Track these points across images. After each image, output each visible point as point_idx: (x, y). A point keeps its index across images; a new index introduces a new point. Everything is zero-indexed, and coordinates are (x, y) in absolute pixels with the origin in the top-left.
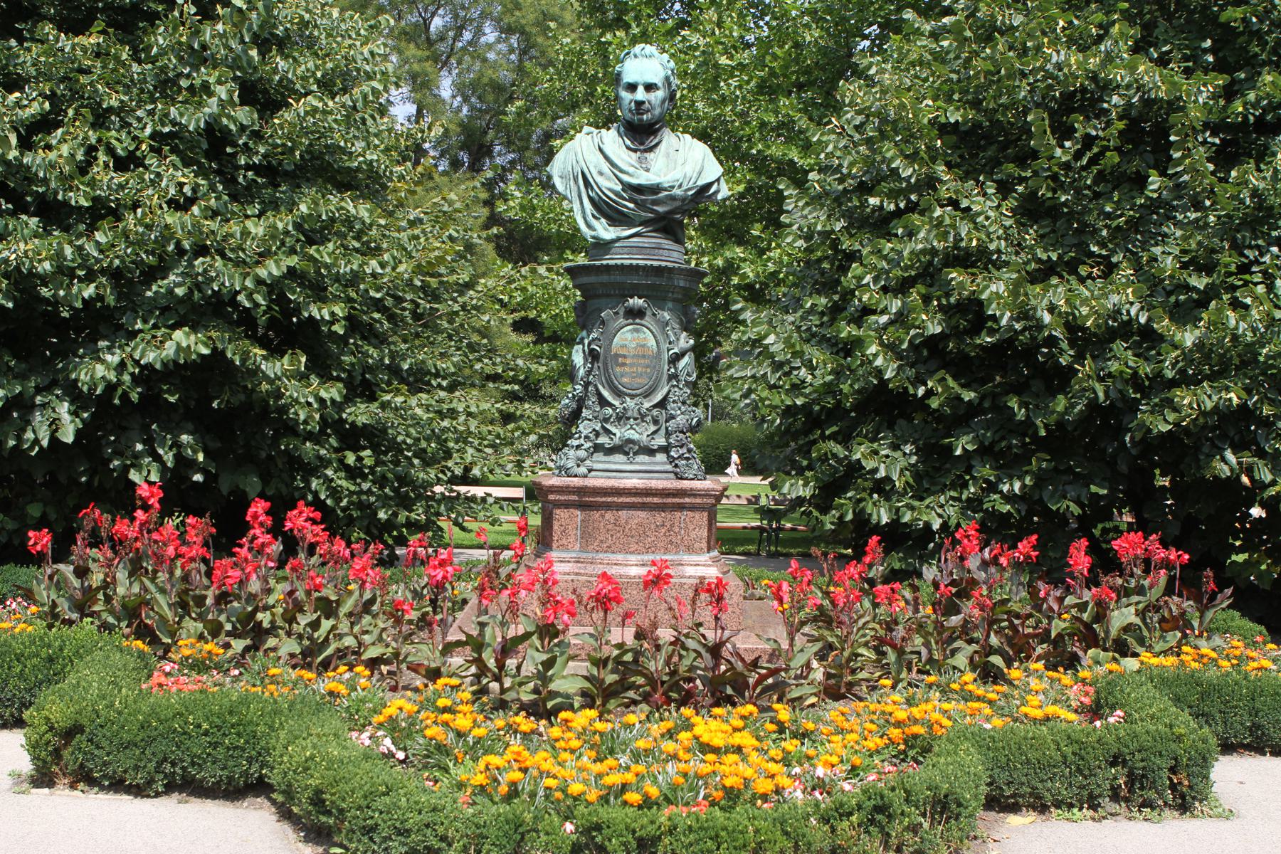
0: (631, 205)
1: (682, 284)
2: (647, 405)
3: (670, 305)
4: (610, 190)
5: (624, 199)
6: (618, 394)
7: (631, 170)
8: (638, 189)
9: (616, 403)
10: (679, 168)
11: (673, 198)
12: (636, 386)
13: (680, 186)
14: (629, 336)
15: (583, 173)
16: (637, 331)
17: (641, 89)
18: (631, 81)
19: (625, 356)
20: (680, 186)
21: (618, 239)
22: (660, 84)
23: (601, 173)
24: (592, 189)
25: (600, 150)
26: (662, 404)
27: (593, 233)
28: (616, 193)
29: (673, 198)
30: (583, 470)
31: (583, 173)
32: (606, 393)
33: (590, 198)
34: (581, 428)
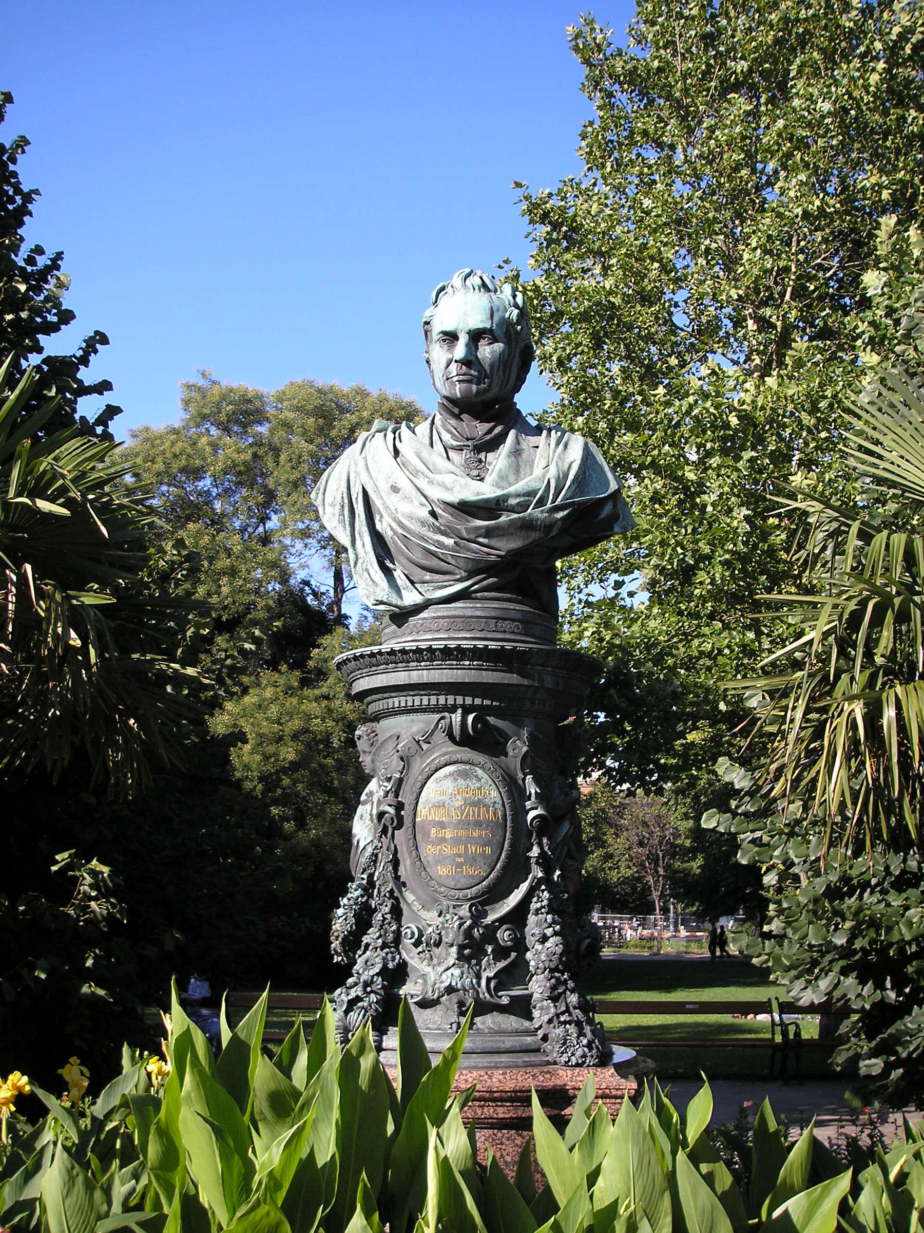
0: (450, 542)
2: (489, 920)
4: (411, 517)
10: (538, 471)
11: (527, 525)
12: (464, 882)
13: (541, 502)
14: (449, 786)
15: (365, 492)
16: (465, 775)
17: (463, 339)
18: (449, 328)
19: (442, 825)
20: (541, 502)
23: (395, 489)
24: (382, 517)
25: (397, 453)
26: (518, 917)
28: (423, 523)
31: (365, 492)
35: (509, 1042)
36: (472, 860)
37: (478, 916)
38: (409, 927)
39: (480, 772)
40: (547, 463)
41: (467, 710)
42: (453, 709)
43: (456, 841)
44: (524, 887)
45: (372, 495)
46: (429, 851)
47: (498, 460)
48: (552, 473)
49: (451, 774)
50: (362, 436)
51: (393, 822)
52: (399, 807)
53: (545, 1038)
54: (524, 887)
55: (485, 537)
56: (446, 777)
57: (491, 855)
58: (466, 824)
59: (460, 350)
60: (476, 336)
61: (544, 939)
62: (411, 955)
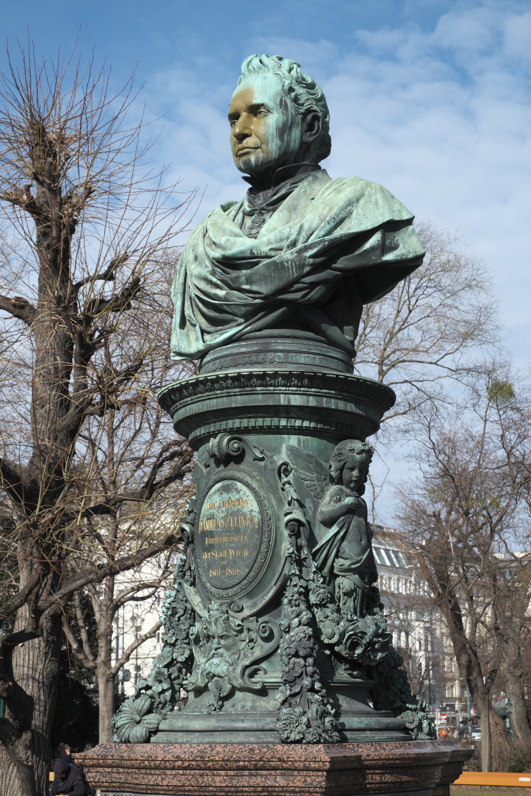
13: (294, 244)
16: (226, 489)
22: (270, 104)
29: (279, 267)
39: (239, 485)
49: (219, 490)
55: (247, 284)
56: (215, 492)
57: (248, 558)
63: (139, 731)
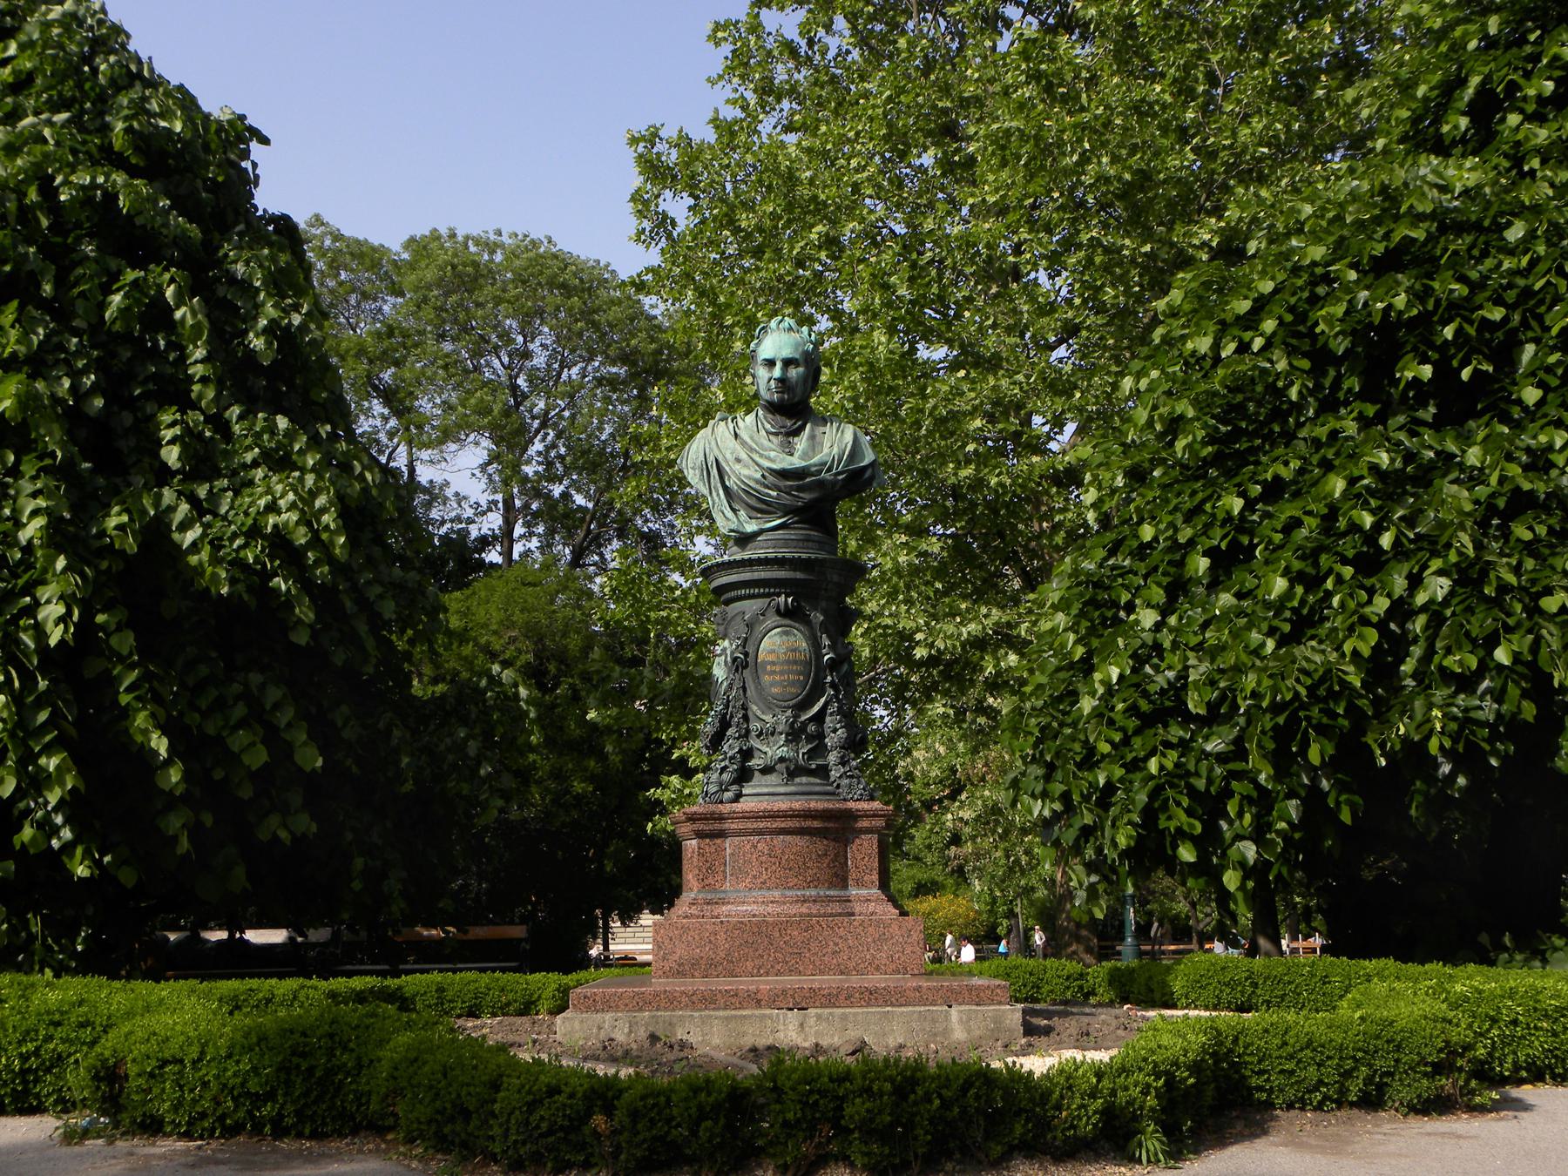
1: (836, 578)
2: (803, 718)
3: (824, 604)
4: (749, 478)
5: (767, 487)
6: (769, 707)
7: (772, 454)
8: (783, 474)
9: (768, 718)
10: (826, 450)
13: (830, 469)
14: (778, 640)
16: (786, 633)
19: (773, 663)
20: (830, 469)
21: (761, 532)
23: (738, 460)
26: (819, 718)
27: (733, 526)
28: (757, 481)
30: (728, 795)
32: (755, 708)
33: (726, 489)
34: (725, 748)
35: (817, 789)
36: (792, 684)
37: (796, 717)
38: (755, 726)
40: (830, 444)
41: (787, 596)
42: (779, 595)
43: (781, 673)
44: (823, 700)
45: (724, 464)
46: (766, 679)
47: (801, 443)
48: (835, 450)
50: (711, 422)
51: (739, 665)
52: (746, 654)
53: (838, 786)
54: (823, 700)
58: (788, 662)
59: (777, 372)
60: (788, 363)
61: (835, 731)
62: (755, 743)
63: (728, 795)
